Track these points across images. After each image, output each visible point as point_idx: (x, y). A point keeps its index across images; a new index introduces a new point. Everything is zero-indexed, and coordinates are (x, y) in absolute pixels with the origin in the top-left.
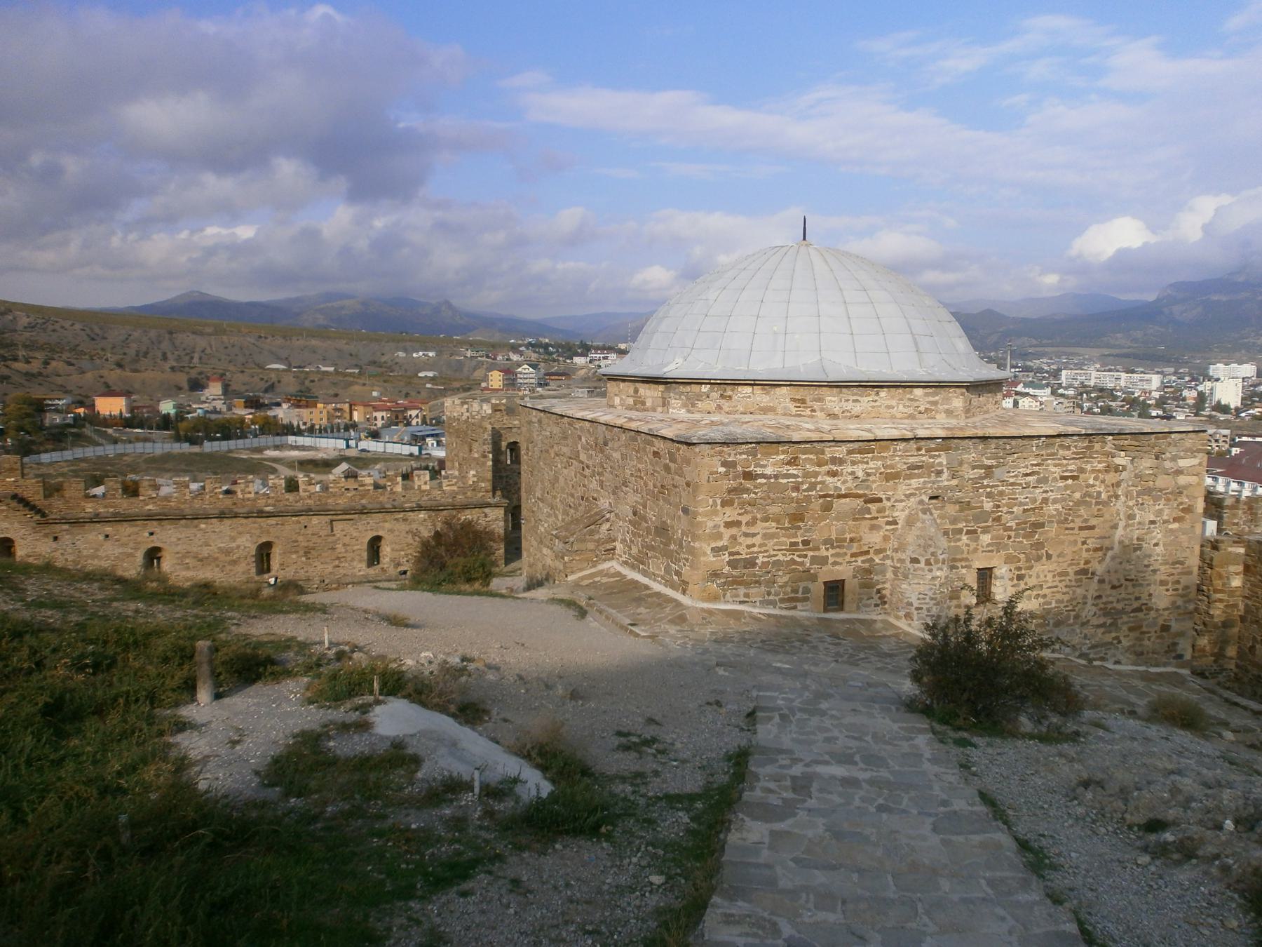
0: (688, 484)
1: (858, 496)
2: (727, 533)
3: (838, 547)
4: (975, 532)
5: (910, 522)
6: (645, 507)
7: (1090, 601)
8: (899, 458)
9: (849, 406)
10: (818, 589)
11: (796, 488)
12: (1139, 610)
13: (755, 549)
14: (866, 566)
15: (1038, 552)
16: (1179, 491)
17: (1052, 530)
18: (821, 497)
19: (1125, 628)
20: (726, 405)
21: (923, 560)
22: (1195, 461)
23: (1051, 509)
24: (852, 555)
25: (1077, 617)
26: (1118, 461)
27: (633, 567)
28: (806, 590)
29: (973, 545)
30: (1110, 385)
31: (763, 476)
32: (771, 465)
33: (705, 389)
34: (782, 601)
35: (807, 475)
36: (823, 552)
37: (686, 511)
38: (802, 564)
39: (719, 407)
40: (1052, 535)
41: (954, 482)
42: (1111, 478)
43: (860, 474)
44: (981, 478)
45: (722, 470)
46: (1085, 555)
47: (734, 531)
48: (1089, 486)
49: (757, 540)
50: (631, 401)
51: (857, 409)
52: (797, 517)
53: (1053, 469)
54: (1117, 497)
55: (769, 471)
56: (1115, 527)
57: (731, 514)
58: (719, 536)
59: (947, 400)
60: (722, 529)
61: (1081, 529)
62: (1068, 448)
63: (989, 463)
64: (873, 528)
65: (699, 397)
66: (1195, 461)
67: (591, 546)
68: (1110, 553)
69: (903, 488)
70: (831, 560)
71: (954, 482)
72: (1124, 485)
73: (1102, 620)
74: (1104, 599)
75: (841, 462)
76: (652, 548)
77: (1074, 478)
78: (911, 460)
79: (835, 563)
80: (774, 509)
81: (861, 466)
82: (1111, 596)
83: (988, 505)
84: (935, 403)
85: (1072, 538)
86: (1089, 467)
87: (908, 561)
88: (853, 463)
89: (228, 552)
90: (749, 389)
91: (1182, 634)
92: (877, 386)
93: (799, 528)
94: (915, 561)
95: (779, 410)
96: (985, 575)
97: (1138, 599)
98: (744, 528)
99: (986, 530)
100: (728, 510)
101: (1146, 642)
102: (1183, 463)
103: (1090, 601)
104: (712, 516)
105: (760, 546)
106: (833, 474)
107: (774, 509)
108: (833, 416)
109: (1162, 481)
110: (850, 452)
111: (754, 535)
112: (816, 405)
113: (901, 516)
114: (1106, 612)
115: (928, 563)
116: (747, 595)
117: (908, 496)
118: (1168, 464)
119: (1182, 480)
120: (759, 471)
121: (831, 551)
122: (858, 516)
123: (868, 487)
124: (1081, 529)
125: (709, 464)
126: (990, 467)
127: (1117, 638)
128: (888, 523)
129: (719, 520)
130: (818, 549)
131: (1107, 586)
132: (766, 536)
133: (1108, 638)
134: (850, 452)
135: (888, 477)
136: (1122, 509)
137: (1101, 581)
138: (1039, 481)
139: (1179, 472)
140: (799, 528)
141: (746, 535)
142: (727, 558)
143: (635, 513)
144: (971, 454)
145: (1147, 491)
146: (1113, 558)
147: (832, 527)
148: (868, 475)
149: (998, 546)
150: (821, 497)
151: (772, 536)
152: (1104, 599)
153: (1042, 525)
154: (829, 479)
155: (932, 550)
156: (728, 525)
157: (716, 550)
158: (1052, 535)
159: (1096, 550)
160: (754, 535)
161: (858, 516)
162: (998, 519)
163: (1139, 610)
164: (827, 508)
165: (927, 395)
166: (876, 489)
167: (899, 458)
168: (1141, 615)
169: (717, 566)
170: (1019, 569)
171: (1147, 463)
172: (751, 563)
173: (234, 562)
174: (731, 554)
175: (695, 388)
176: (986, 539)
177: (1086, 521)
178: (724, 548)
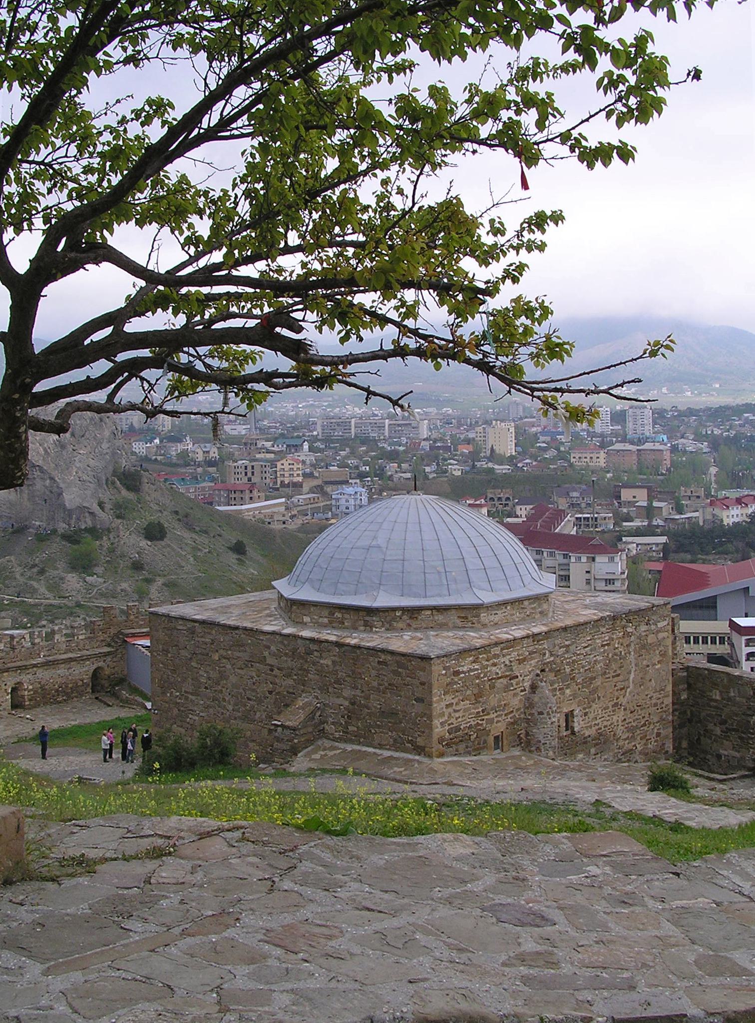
0: (423, 684)
1: (507, 676)
2: (447, 712)
3: (500, 711)
4: (562, 689)
5: (534, 688)
6: (367, 698)
7: (620, 723)
8: (523, 650)
9: (492, 618)
11: (478, 677)
12: (645, 725)
13: (460, 720)
14: (512, 720)
15: (592, 697)
16: (660, 643)
17: (598, 682)
18: (489, 680)
19: (639, 738)
20: (414, 624)
21: (545, 712)
22: (665, 623)
23: (598, 666)
24: (506, 715)
25: (614, 735)
26: (629, 630)
27: (351, 742)
28: (485, 742)
29: (562, 697)
31: (463, 672)
32: (466, 665)
33: (398, 614)
34: (474, 750)
35: (484, 667)
36: (492, 716)
37: (420, 700)
38: (482, 725)
39: (409, 625)
40: (599, 683)
41: (552, 659)
42: (626, 641)
43: (507, 663)
44: (564, 653)
45: (444, 672)
46: (616, 694)
47: (450, 710)
48: (616, 648)
49: (460, 714)
50: (326, 620)
51: (496, 619)
52: (478, 696)
53: (598, 641)
54: (630, 653)
55: (465, 669)
56: (630, 673)
57: (449, 699)
58: (442, 714)
59: (540, 605)
60: (444, 710)
61: (613, 677)
62: (604, 626)
63: (567, 643)
64: (515, 695)
65: (394, 619)
66: (665, 623)
67: (310, 729)
68: (628, 690)
70: (496, 720)
71: (552, 659)
72: (632, 645)
73: (627, 735)
74: (627, 721)
75: (496, 656)
76: (379, 727)
77: (608, 645)
78: (531, 649)
79: (498, 722)
80: (469, 692)
81: (508, 657)
83: (568, 671)
84: (533, 608)
85: (609, 684)
86: (615, 636)
87: (536, 714)
88: (504, 656)
90: (429, 612)
91: (667, 737)
92: (505, 603)
93: (480, 702)
94: (541, 713)
95: (450, 625)
97: (644, 717)
98: (454, 707)
99: (568, 687)
100: (448, 697)
101: (650, 746)
102: (660, 625)
103: (620, 723)
104: (440, 702)
105: (463, 716)
106: (494, 665)
107: (469, 692)
108: (484, 626)
109: (651, 639)
110: (502, 649)
111: (458, 711)
112: (475, 620)
113: (527, 684)
114: (629, 730)
115: (548, 714)
116: (457, 750)
117: (530, 672)
118: (653, 627)
119: (661, 635)
120: (461, 669)
121: (496, 714)
122: (506, 689)
123: (512, 670)
124: (613, 677)
125: (437, 669)
126: (568, 646)
127: (635, 745)
128: (522, 691)
129: (443, 704)
130: (488, 714)
131: (628, 712)
132: (465, 710)
133: (630, 746)
134: (502, 649)
135: (520, 662)
136: (633, 661)
137: (625, 710)
138: (591, 650)
139: (658, 632)
140: (480, 702)
141: (455, 711)
142: (447, 728)
143: (353, 704)
145: (643, 647)
146: (630, 693)
147: (493, 700)
148: (511, 662)
149: (574, 696)
150: (489, 680)
151: (469, 709)
152: (627, 721)
153: (595, 678)
154: (494, 668)
155: (549, 705)
156: (447, 706)
157: (442, 724)
158: (599, 683)
159: (621, 689)
160: (458, 711)
161: (506, 689)
162: (573, 679)
163: (645, 725)
164: (492, 687)
165: (530, 604)
167: (523, 650)
168: (645, 728)
169: (442, 734)
170: (585, 709)
172: (458, 729)
174: (449, 725)
175: (392, 614)
176: (568, 691)
177: (615, 671)
178: (446, 721)
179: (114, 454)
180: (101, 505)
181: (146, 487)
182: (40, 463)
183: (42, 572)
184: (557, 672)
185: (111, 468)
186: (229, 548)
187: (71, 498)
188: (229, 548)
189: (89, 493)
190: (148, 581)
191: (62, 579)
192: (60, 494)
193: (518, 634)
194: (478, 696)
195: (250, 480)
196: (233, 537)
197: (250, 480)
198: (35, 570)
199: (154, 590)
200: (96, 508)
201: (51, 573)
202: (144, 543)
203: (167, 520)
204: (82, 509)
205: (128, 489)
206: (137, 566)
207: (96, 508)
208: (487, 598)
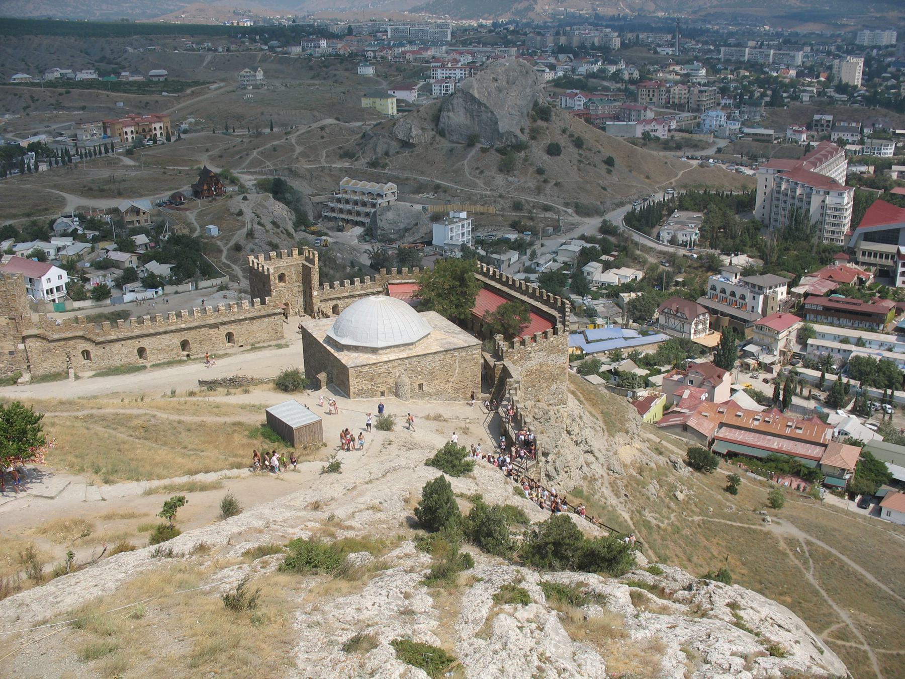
10: (379, 393)
15: (434, 378)
30: (761, 61)
32: (365, 369)
52: (372, 380)
57: (357, 380)
69: (397, 369)
82: (456, 386)
89: (169, 346)
92: (391, 347)
96: (421, 386)
125: (351, 371)
144: (414, 359)
161: (386, 377)
166: (391, 370)
167: (396, 363)
171: (464, 354)
173: (172, 350)
179: (533, 96)
180: (522, 130)
181: (553, 118)
182: (485, 102)
183: (482, 172)
184: (413, 371)
185: (531, 105)
186: (604, 161)
187: (503, 126)
188: (604, 161)
189: (515, 122)
190: (545, 181)
191: (494, 178)
192: (496, 123)
193: (394, 358)
194: (372, 380)
195: (651, 99)
196: (607, 153)
197: (651, 99)
198: (478, 171)
199: (548, 188)
200: (518, 133)
201: (487, 173)
202: (546, 157)
203: (563, 141)
204: (509, 133)
205: (542, 119)
206: (540, 171)
207: (518, 133)
208: (380, 344)
